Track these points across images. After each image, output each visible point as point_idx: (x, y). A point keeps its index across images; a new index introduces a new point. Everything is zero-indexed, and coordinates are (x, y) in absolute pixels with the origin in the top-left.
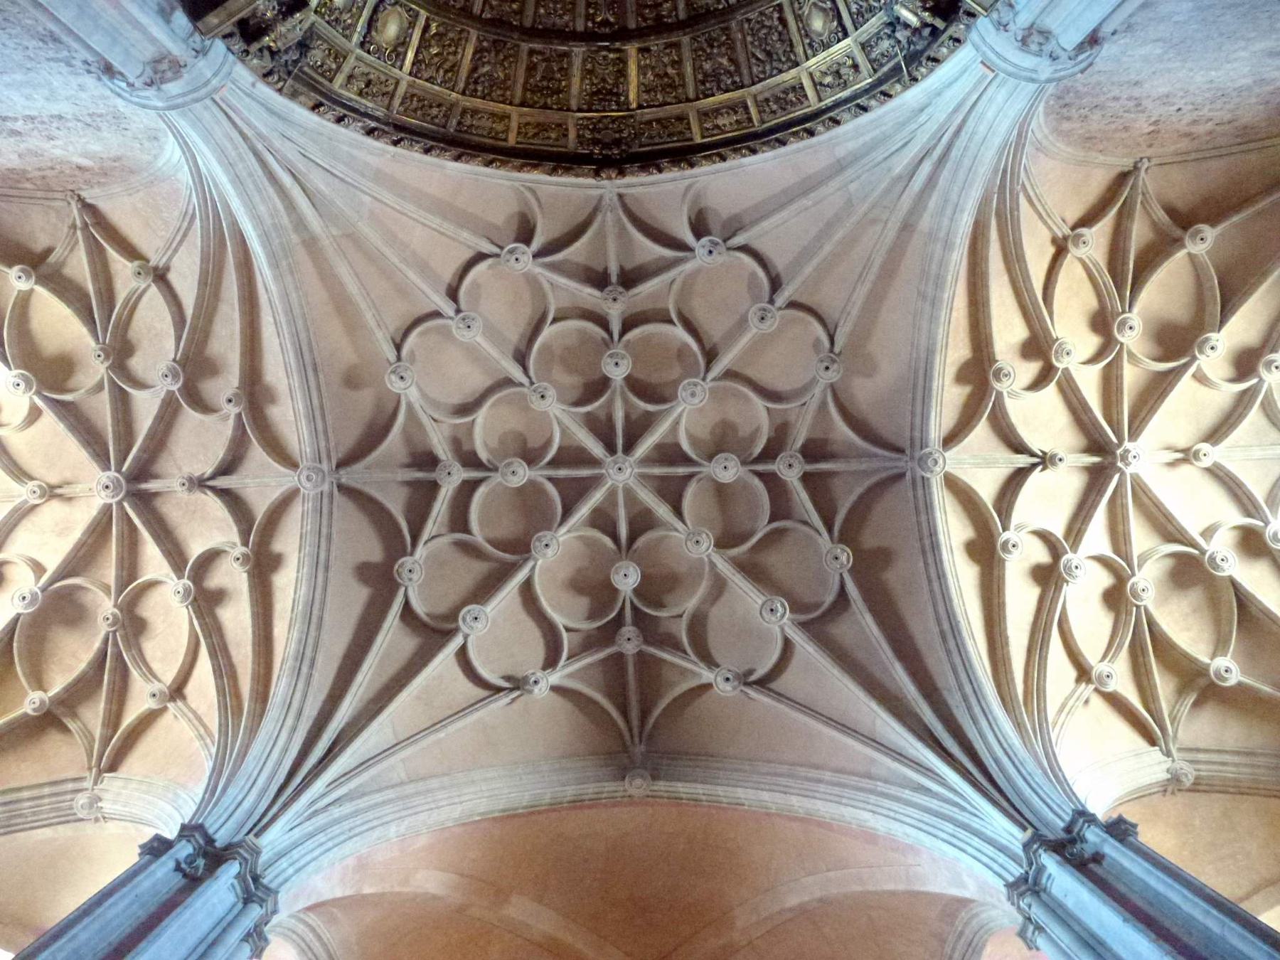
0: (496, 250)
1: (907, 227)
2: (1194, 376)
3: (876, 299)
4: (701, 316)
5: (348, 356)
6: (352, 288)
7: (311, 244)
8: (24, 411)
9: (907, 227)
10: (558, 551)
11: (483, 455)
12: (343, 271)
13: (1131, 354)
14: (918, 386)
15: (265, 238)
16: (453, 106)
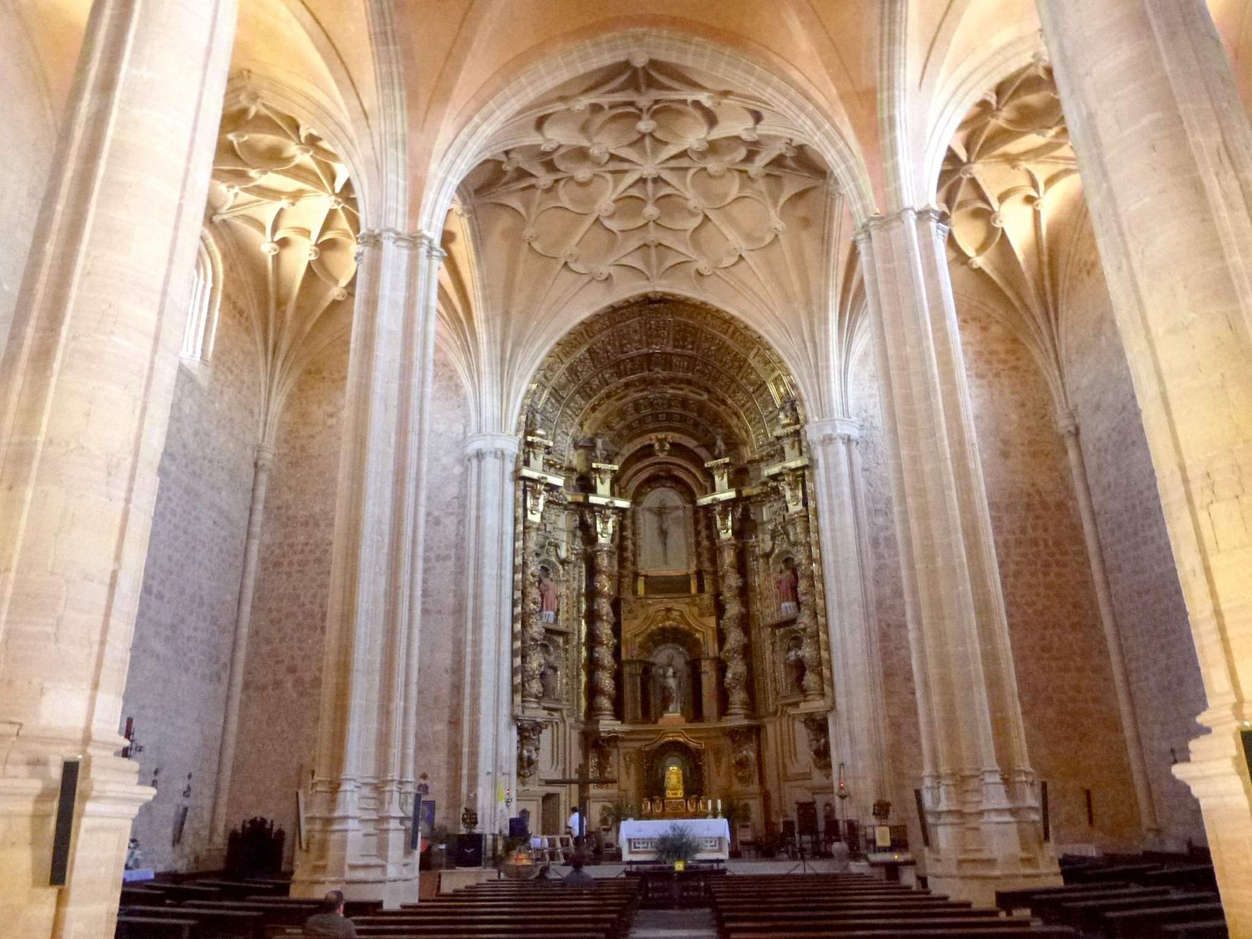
0: (718, 272)
1: (507, 314)
2: (309, 232)
3: (511, 270)
4: (604, 236)
5: (804, 236)
6: (794, 276)
7: (808, 302)
8: (1008, 203)
9: (507, 314)
10: (694, 136)
11: (736, 174)
12: (797, 287)
13: (349, 237)
14: (479, 239)
15: (825, 321)
16: (731, 337)
